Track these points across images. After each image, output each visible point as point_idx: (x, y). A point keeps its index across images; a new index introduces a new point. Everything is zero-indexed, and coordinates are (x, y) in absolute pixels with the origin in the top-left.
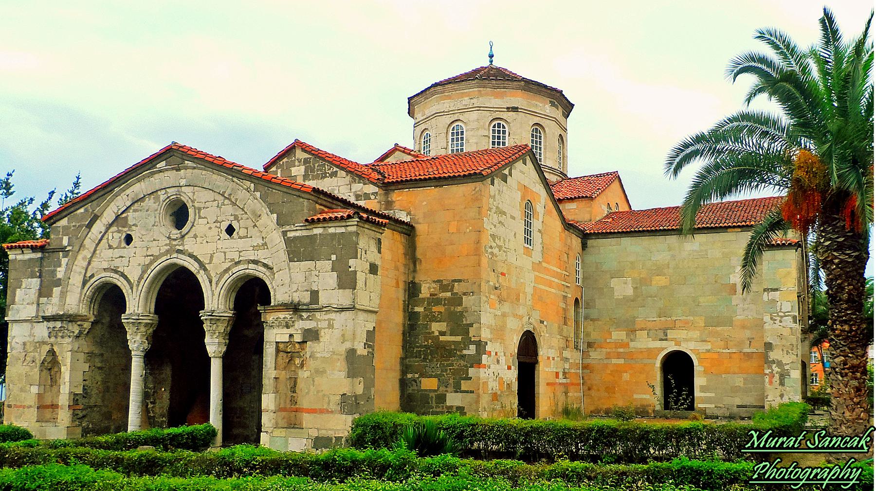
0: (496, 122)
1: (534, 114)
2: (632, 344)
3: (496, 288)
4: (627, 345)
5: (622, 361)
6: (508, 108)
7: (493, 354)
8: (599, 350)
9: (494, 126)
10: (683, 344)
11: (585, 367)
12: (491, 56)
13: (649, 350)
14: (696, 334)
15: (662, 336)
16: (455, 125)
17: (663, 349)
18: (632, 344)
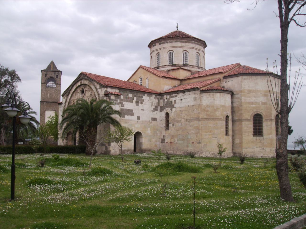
12: (177, 27)
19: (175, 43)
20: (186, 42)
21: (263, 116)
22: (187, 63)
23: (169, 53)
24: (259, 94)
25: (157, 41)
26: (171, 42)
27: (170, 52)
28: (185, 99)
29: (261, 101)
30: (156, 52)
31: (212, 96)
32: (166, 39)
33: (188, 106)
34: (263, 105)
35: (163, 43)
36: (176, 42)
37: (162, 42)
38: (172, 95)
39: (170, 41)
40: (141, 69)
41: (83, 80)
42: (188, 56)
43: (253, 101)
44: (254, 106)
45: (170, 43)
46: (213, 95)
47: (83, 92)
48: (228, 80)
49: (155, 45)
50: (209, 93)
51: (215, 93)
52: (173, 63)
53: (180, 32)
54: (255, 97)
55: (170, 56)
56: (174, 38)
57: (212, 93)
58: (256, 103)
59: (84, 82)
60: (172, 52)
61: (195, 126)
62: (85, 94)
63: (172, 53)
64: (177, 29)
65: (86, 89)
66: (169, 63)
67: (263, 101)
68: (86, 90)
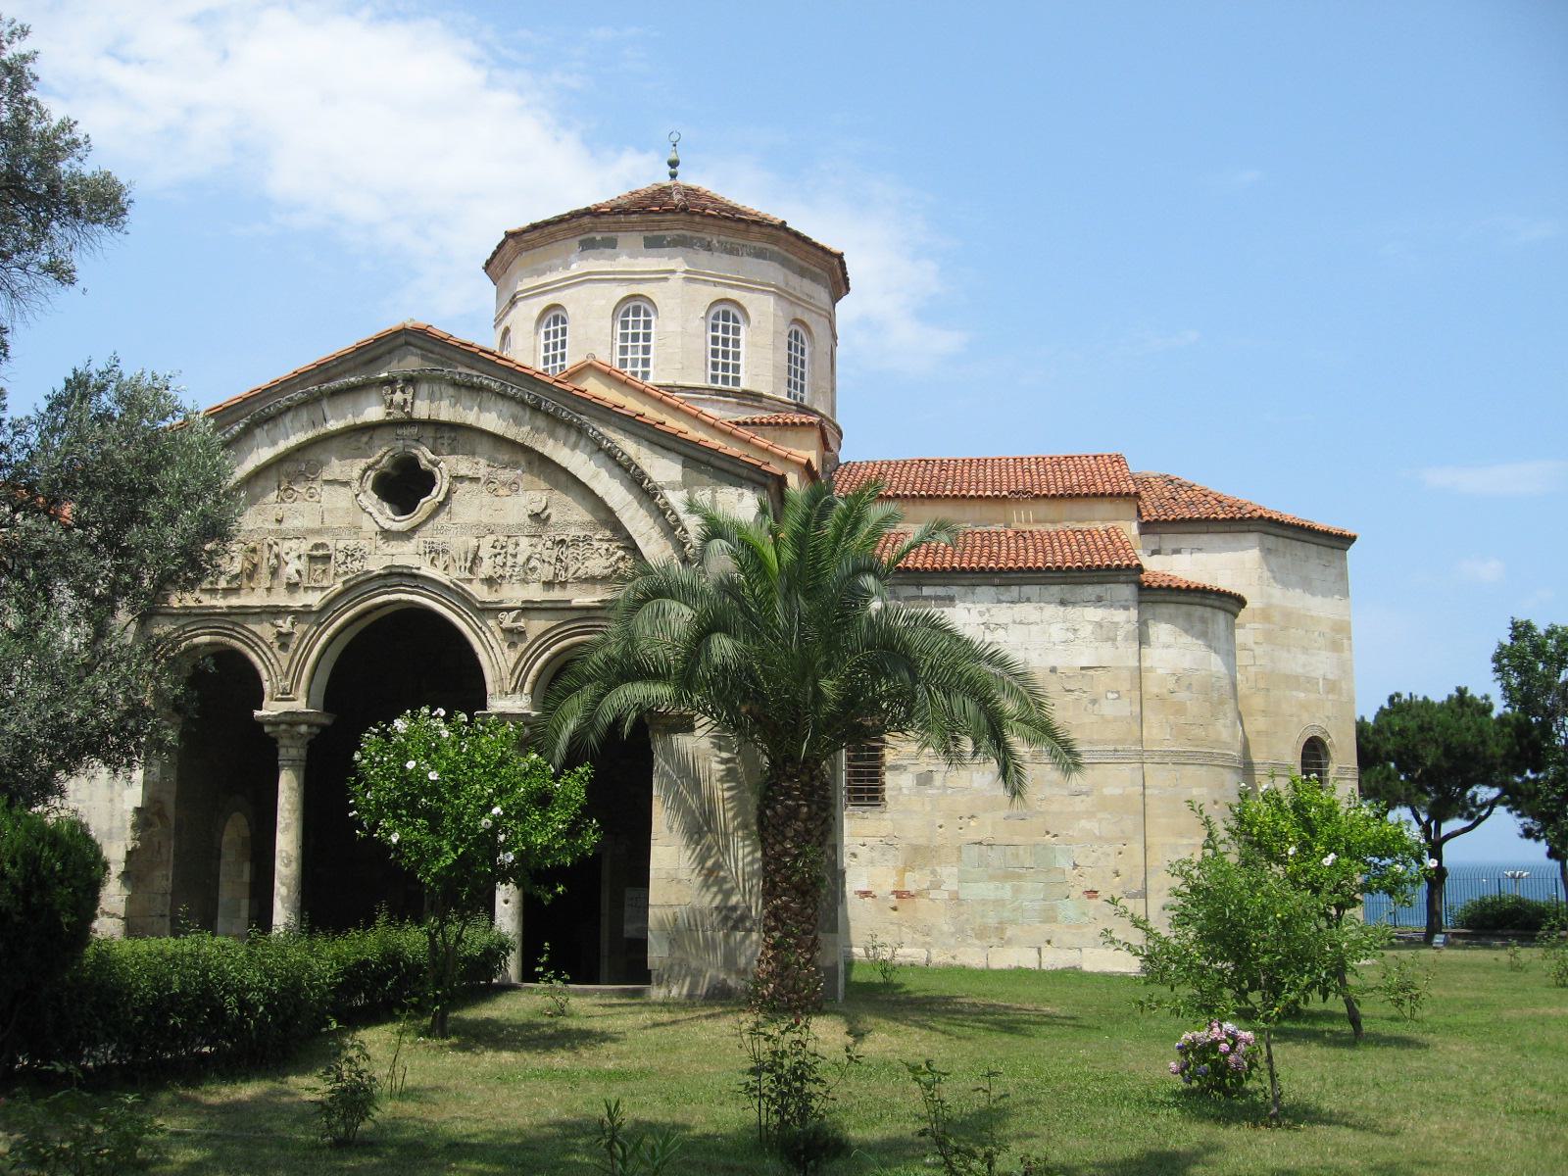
19: (755, 260)
20: (802, 273)
21: (1332, 753)
22: (802, 399)
23: (716, 317)
24: (1316, 634)
25: (634, 218)
26: (732, 251)
27: (721, 308)
28: (1021, 623)
29: (1322, 672)
30: (623, 291)
31: (1198, 626)
32: (710, 221)
33: (1053, 670)
34: (1330, 697)
36: (760, 254)
37: (670, 235)
38: (912, 591)
39: (722, 238)
41: (424, 389)
42: (806, 357)
43: (1300, 670)
44: (1302, 695)
45: (726, 259)
46: (1203, 620)
47: (404, 486)
48: (1169, 541)
49: (611, 244)
50: (1184, 608)
51: (1209, 609)
52: (736, 381)
53: (690, 192)
54: (1305, 650)
55: (720, 334)
56: (755, 229)
57: (1198, 611)
58: (1309, 680)
60: (733, 310)
61: (1107, 791)
62: (442, 505)
63: (736, 320)
64: (673, 176)
65: (447, 466)
66: (714, 378)
67: (1330, 676)
68: (462, 473)
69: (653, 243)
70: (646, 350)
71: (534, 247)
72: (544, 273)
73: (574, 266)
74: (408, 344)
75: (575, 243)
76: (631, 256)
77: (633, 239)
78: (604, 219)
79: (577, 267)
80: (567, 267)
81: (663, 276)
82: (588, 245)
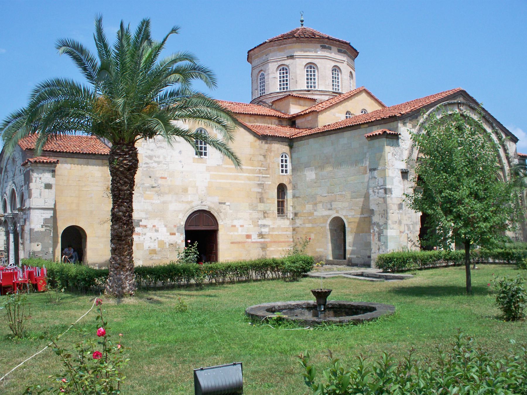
0: (281, 67)
1: (307, 57)
2: (315, 213)
3: (153, 187)
4: (311, 214)
5: (310, 225)
6: (287, 57)
7: (150, 226)
8: (300, 218)
9: (280, 70)
10: (340, 213)
11: (294, 230)
13: (323, 216)
14: (346, 204)
15: (329, 206)
16: (261, 74)
17: (330, 216)
18: (315, 213)
35: (345, 53)
40: (364, 95)
49: (330, 49)
59: (468, 113)
64: (302, 25)
69: (340, 51)
70: (338, 82)
71: (302, 42)
72: (306, 52)
73: (319, 52)
74: (461, 94)
75: (319, 45)
76: (335, 54)
77: (335, 49)
78: (331, 41)
79: (320, 53)
80: (316, 52)
81: (342, 62)
82: (323, 47)
